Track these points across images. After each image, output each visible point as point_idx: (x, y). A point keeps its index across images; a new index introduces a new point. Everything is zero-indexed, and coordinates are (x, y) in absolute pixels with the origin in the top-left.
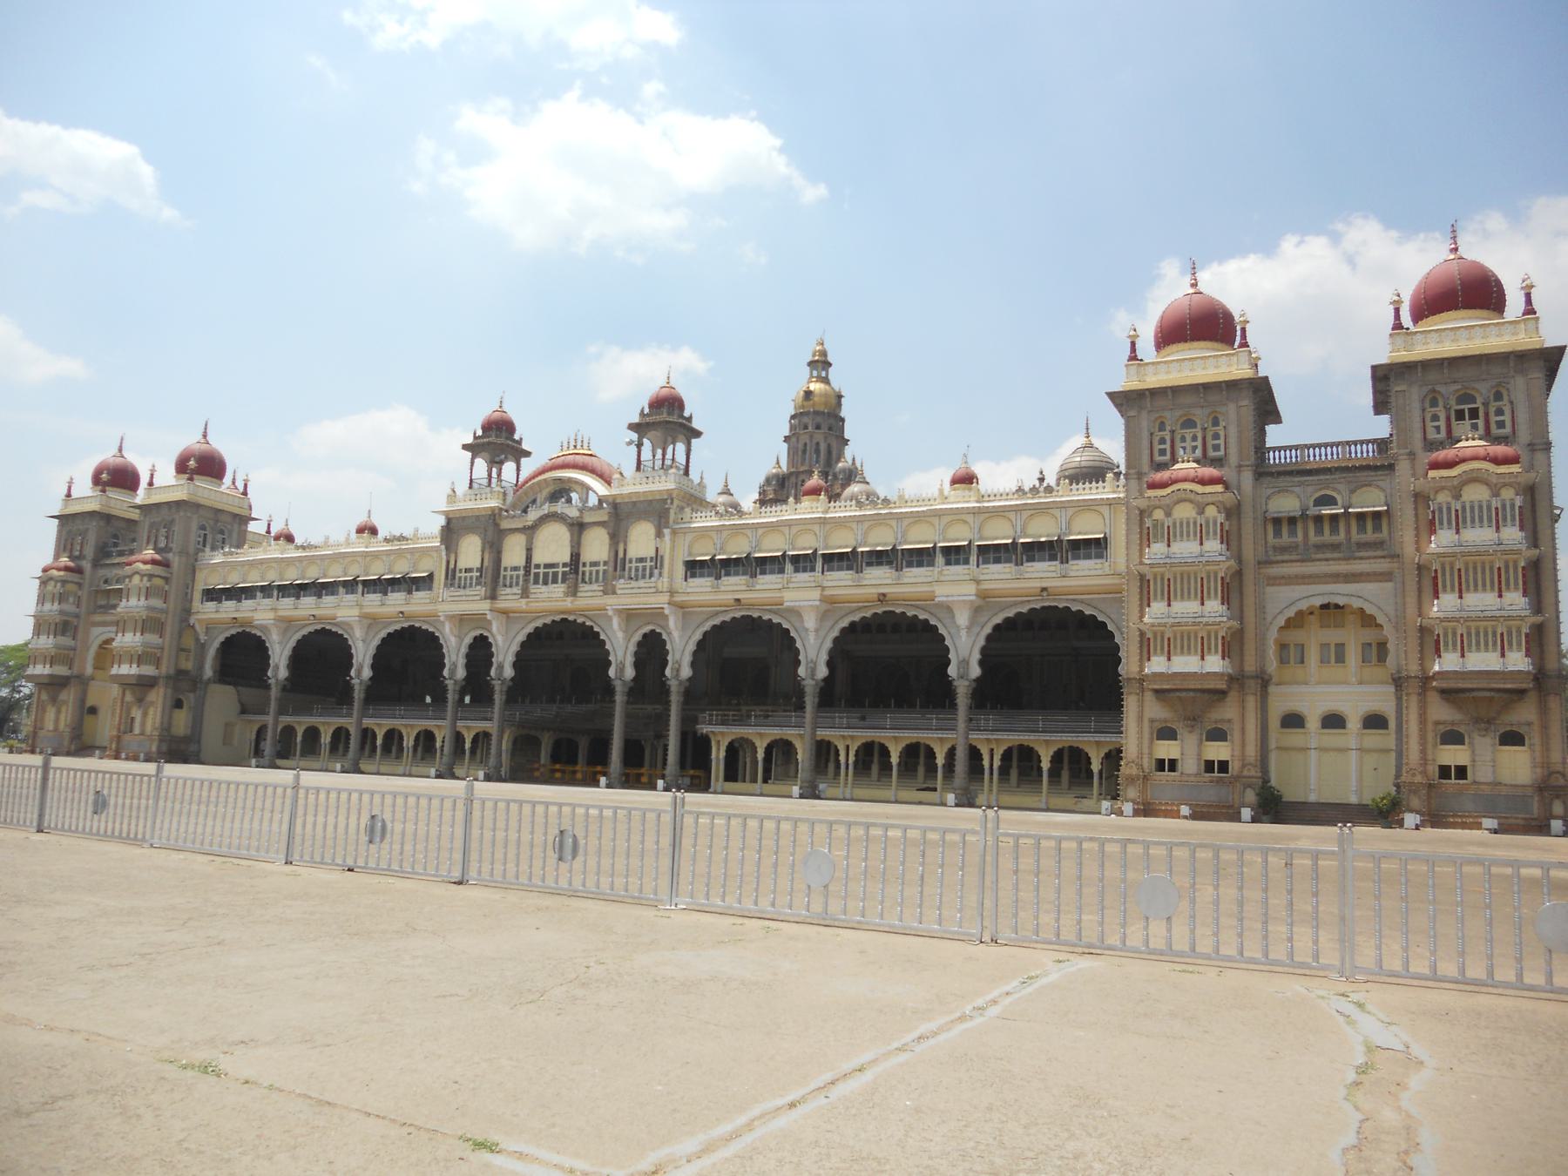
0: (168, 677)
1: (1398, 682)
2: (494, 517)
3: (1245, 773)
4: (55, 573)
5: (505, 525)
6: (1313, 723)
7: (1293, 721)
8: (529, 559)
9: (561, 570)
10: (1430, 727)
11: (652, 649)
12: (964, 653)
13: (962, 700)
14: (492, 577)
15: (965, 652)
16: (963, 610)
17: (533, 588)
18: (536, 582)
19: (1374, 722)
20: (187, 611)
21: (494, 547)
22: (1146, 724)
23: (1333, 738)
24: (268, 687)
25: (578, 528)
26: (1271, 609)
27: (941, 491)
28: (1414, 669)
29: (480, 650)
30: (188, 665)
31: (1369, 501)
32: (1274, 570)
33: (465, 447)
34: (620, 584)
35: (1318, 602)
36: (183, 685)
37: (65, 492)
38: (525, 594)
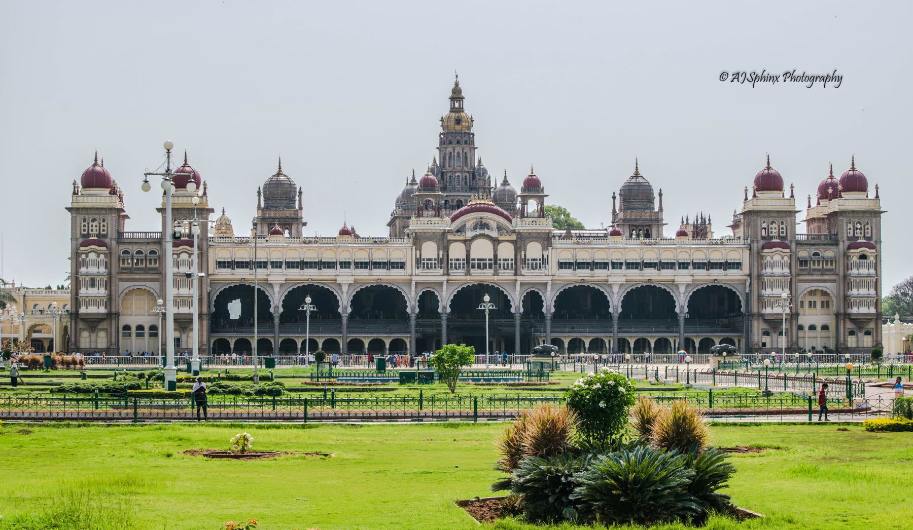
1: (837, 315)
2: (444, 234)
5: (450, 237)
6: (806, 329)
7: (801, 328)
8: (468, 255)
9: (488, 262)
11: (533, 300)
12: (682, 303)
14: (444, 262)
15: (682, 302)
16: (683, 285)
17: (472, 271)
18: (473, 267)
19: (825, 328)
23: (812, 333)
25: (496, 242)
26: (799, 291)
28: (842, 311)
29: (428, 299)
31: (829, 253)
32: (801, 277)
34: (524, 271)
35: (813, 289)
38: (468, 273)
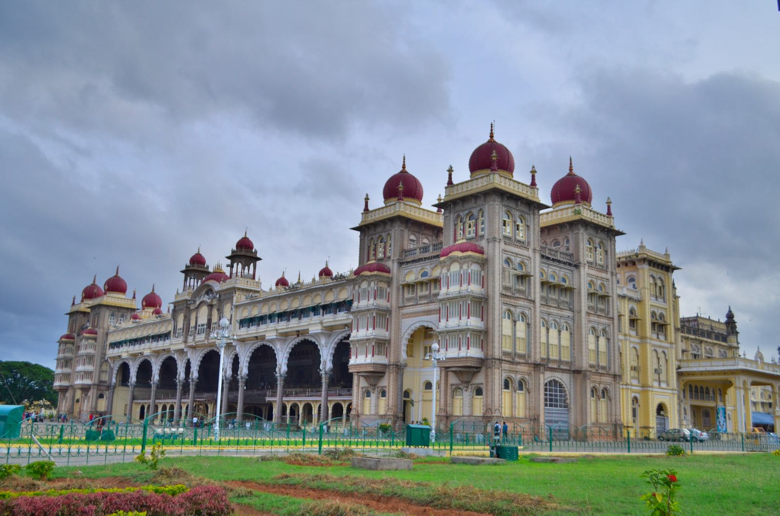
0: (94, 385)
3: (388, 413)
4: (63, 339)
10: (449, 387)
12: (325, 358)
13: (324, 381)
20: (104, 354)
21: (187, 319)
22: (360, 390)
24: (150, 386)
25: (211, 306)
26: (403, 331)
27: (314, 280)
30: (105, 377)
32: (405, 311)
33: (183, 272)
36: (103, 389)
37: (72, 302)
38: (194, 339)
